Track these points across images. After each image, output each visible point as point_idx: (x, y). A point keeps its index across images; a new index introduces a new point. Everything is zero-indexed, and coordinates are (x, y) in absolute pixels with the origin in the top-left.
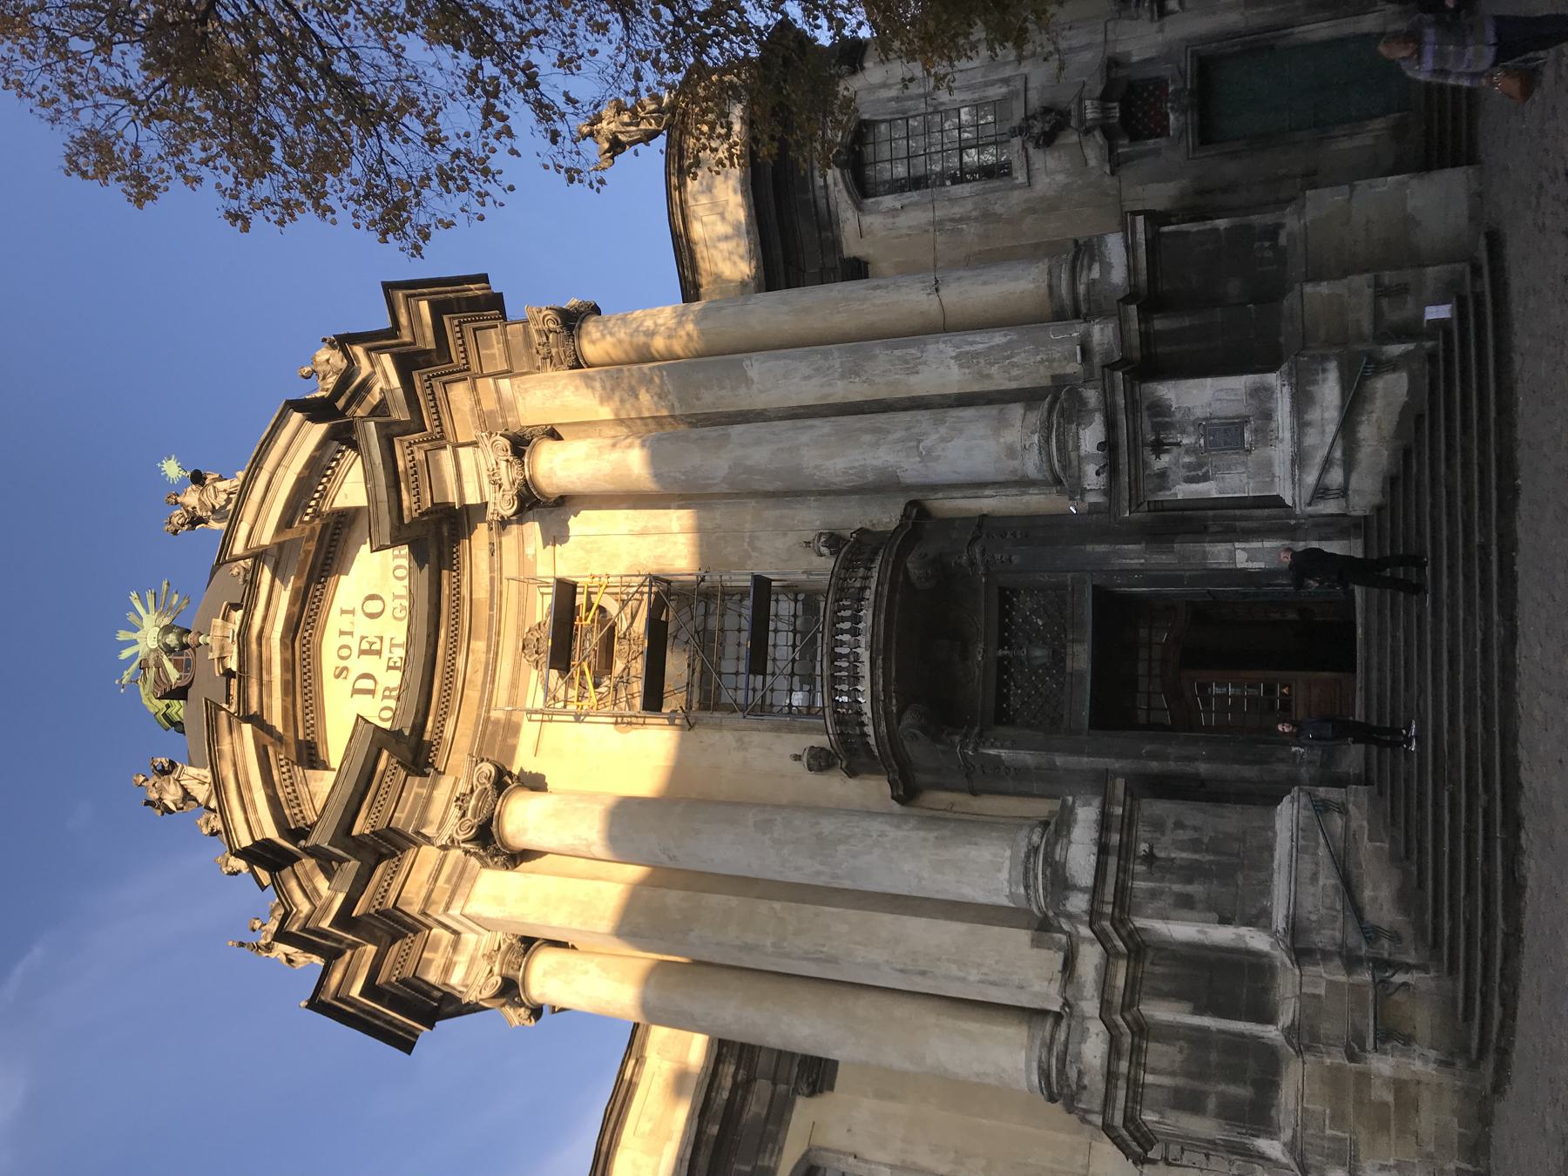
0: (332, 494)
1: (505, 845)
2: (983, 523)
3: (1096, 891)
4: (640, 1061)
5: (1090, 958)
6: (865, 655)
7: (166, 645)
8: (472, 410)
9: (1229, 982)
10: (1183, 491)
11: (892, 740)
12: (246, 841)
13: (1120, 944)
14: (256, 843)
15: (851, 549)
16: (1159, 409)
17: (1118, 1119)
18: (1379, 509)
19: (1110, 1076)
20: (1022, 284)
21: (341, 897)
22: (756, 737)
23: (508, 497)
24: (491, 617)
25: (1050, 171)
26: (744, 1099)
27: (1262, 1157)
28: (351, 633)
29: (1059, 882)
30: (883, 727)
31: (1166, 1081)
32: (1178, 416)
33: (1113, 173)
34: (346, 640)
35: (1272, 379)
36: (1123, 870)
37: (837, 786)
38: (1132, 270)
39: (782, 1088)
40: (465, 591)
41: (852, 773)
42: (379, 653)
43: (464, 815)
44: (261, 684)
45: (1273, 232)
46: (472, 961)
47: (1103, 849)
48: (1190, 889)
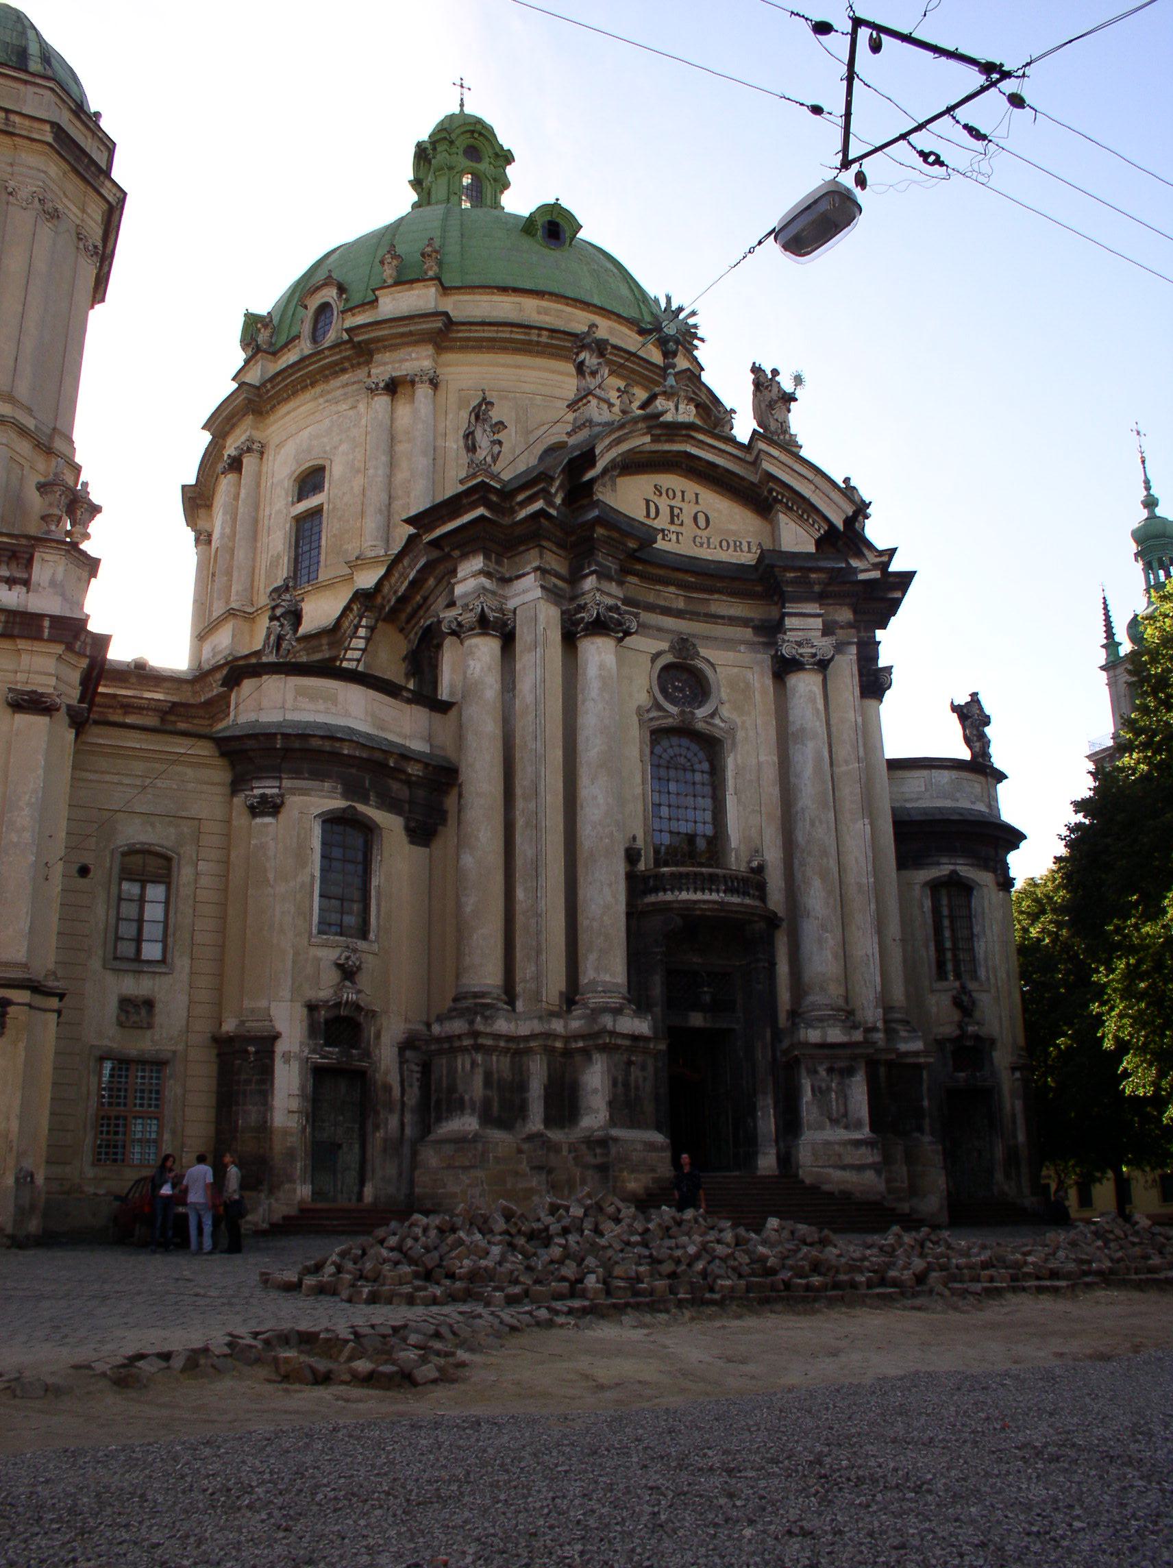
0: (789, 513)
1: (585, 636)
2: (773, 964)
3: (613, 1033)
4: (409, 701)
5: (557, 1026)
6: (714, 897)
7: (668, 341)
8: (836, 622)
9: (564, 1102)
10: (807, 1085)
11: (666, 907)
12: (597, 452)
13: (581, 1044)
14: (594, 456)
15: (754, 881)
16: (850, 1072)
17: (480, 1041)
18: (803, 1182)
19: (497, 1037)
20: (898, 994)
21: (554, 512)
22: (640, 807)
23: (794, 651)
24: (698, 614)
25: (939, 1004)
26: (401, 781)
27: (439, 1120)
28: (683, 500)
29: (617, 1011)
30: (675, 905)
31: (495, 1067)
32: (847, 1081)
33: (936, 1040)
34: (679, 494)
35: (867, 1129)
36: (628, 1049)
37: (621, 867)
38: (907, 1054)
39: (407, 807)
40: (716, 596)
41: (631, 877)
42: (672, 522)
43: (610, 609)
44: (660, 435)
45: (920, 1129)
46: (493, 593)
47: (635, 1038)
48: (620, 1085)
